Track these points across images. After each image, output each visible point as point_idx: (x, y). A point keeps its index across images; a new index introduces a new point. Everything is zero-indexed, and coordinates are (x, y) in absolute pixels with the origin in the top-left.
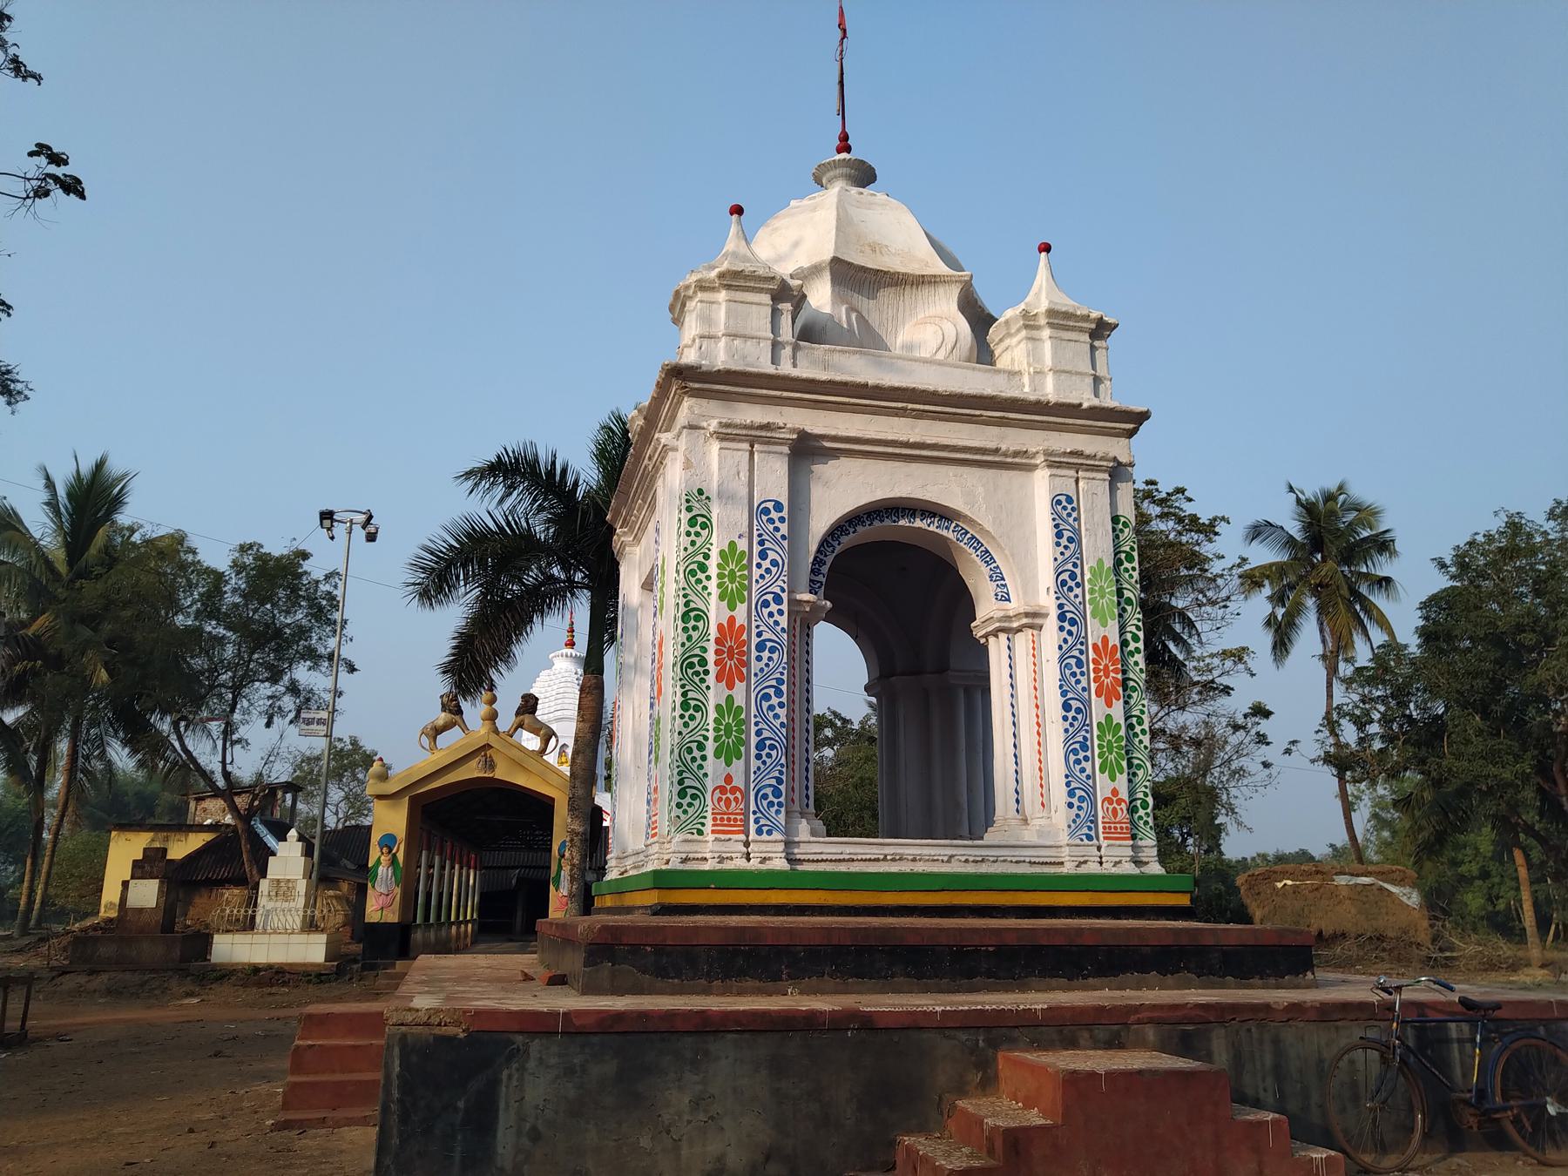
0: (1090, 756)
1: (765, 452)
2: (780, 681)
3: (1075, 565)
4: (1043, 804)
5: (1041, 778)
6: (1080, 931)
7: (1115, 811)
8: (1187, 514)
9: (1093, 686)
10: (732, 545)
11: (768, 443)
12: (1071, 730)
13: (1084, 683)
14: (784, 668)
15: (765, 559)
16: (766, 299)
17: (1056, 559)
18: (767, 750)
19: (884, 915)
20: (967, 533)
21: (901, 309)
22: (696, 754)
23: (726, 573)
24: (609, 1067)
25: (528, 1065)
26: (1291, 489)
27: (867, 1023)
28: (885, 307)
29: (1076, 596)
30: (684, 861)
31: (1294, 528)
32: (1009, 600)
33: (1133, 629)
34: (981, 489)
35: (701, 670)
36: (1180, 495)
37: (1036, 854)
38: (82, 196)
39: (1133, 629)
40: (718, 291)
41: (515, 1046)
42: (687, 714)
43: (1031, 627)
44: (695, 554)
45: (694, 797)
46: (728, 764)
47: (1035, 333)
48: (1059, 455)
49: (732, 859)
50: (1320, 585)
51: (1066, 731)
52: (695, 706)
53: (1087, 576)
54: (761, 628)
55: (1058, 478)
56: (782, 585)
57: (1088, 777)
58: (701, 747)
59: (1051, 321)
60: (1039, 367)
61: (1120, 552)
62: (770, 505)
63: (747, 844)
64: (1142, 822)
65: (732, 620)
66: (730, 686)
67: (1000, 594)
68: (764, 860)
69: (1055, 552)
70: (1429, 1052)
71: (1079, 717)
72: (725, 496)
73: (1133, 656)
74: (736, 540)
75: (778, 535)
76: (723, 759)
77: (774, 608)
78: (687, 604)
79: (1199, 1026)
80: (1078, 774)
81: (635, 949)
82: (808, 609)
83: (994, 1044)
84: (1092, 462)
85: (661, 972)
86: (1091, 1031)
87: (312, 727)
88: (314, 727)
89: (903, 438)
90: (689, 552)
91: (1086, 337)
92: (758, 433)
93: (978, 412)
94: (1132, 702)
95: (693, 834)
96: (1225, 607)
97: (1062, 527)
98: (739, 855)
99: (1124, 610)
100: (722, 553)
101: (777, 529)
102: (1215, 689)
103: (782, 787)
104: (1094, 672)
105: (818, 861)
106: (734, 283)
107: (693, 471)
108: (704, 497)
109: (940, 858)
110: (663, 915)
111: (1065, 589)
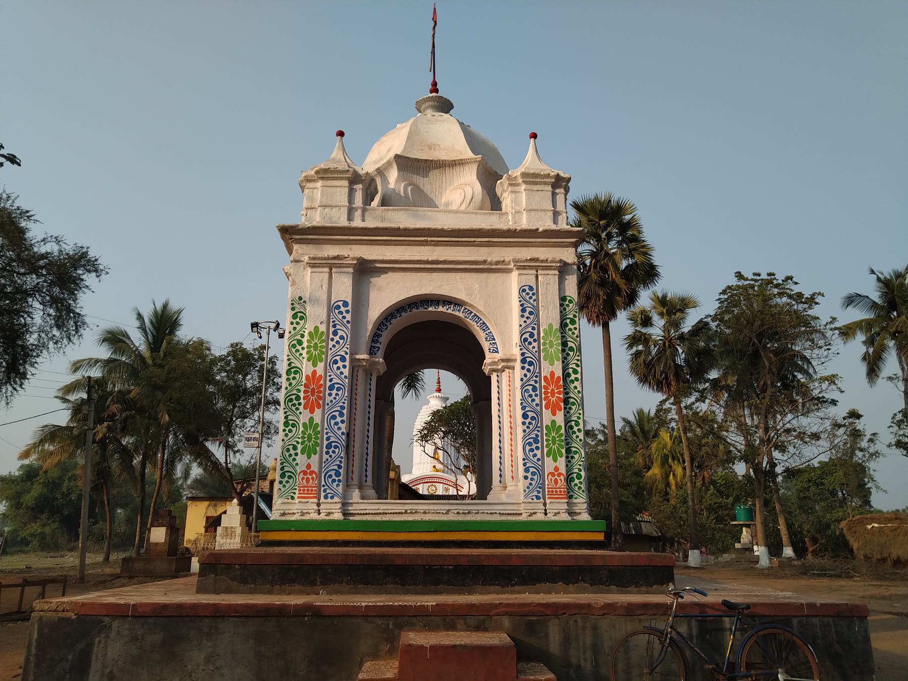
0: (540, 446)
1: (339, 272)
2: (342, 408)
3: (533, 328)
4: (512, 477)
5: (512, 461)
6: (510, 556)
8: (795, 292)
9: (544, 403)
10: (316, 328)
11: (340, 267)
12: (528, 430)
14: (345, 400)
15: (336, 335)
16: (345, 183)
17: (521, 326)
18: (333, 449)
19: (398, 546)
20: (471, 312)
21: (444, 181)
22: (292, 452)
23: (312, 345)
24: (158, 637)
25: (110, 635)
26: (873, 272)
27: (316, 612)
28: (434, 181)
29: (534, 347)
30: (284, 514)
31: (875, 294)
33: (574, 366)
34: (477, 286)
35: (297, 403)
36: (790, 281)
37: (503, 508)
38: (19, 165)
39: (574, 366)
40: (318, 182)
41: (104, 624)
42: (287, 429)
43: (508, 368)
44: (296, 335)
45: (290, 477)
46: (309, 457)
47: (516, 188)
48: (524, 262)
49: (309, 514)
50: (896, 332)
51: (524, 431)
52: (293, 424)
53: (542, 334)
54: (332, 377)
56: (346, 350)
57: (538, 460)
58: (295, 448)
59: (525, 180)
62: (340, 304)
63: (319, 505)
64: (577, 487)
65: (314, 373)
66: (312, 412)
67: (492, 349)
68: (329, 514)
69: (520, 321)
70: (708, 637)
71: (534, 422)
72: (315, 301)
73: (573, 383)
74: (319, 325)
75: (345, 321)
76: (306, 454)
77: (340, 364)
78: (289, 365)
80: (532, 458)
81: (229, 566)
82: (364, 364)
83: (400, 627)
84: (545, 264)
85: (244, 581)
86: (464, 619)
87: (250, 442)
88: (252, 442)
89: (425, 258)
90: (292, 334)
91: (549, 188)
92: (333, 262)
93: (472, 239)
95: (288, 499)
96: (829, 349)
97: (525, 306)
98: (313, 511)
99: (568, 354)
100: (310, 333)
101: (344, 317)
102: (825, 402)
103: (341, 471)
105: (364, 514)
108: (302, 301)
109: (441, 511)
111: (526, 343)
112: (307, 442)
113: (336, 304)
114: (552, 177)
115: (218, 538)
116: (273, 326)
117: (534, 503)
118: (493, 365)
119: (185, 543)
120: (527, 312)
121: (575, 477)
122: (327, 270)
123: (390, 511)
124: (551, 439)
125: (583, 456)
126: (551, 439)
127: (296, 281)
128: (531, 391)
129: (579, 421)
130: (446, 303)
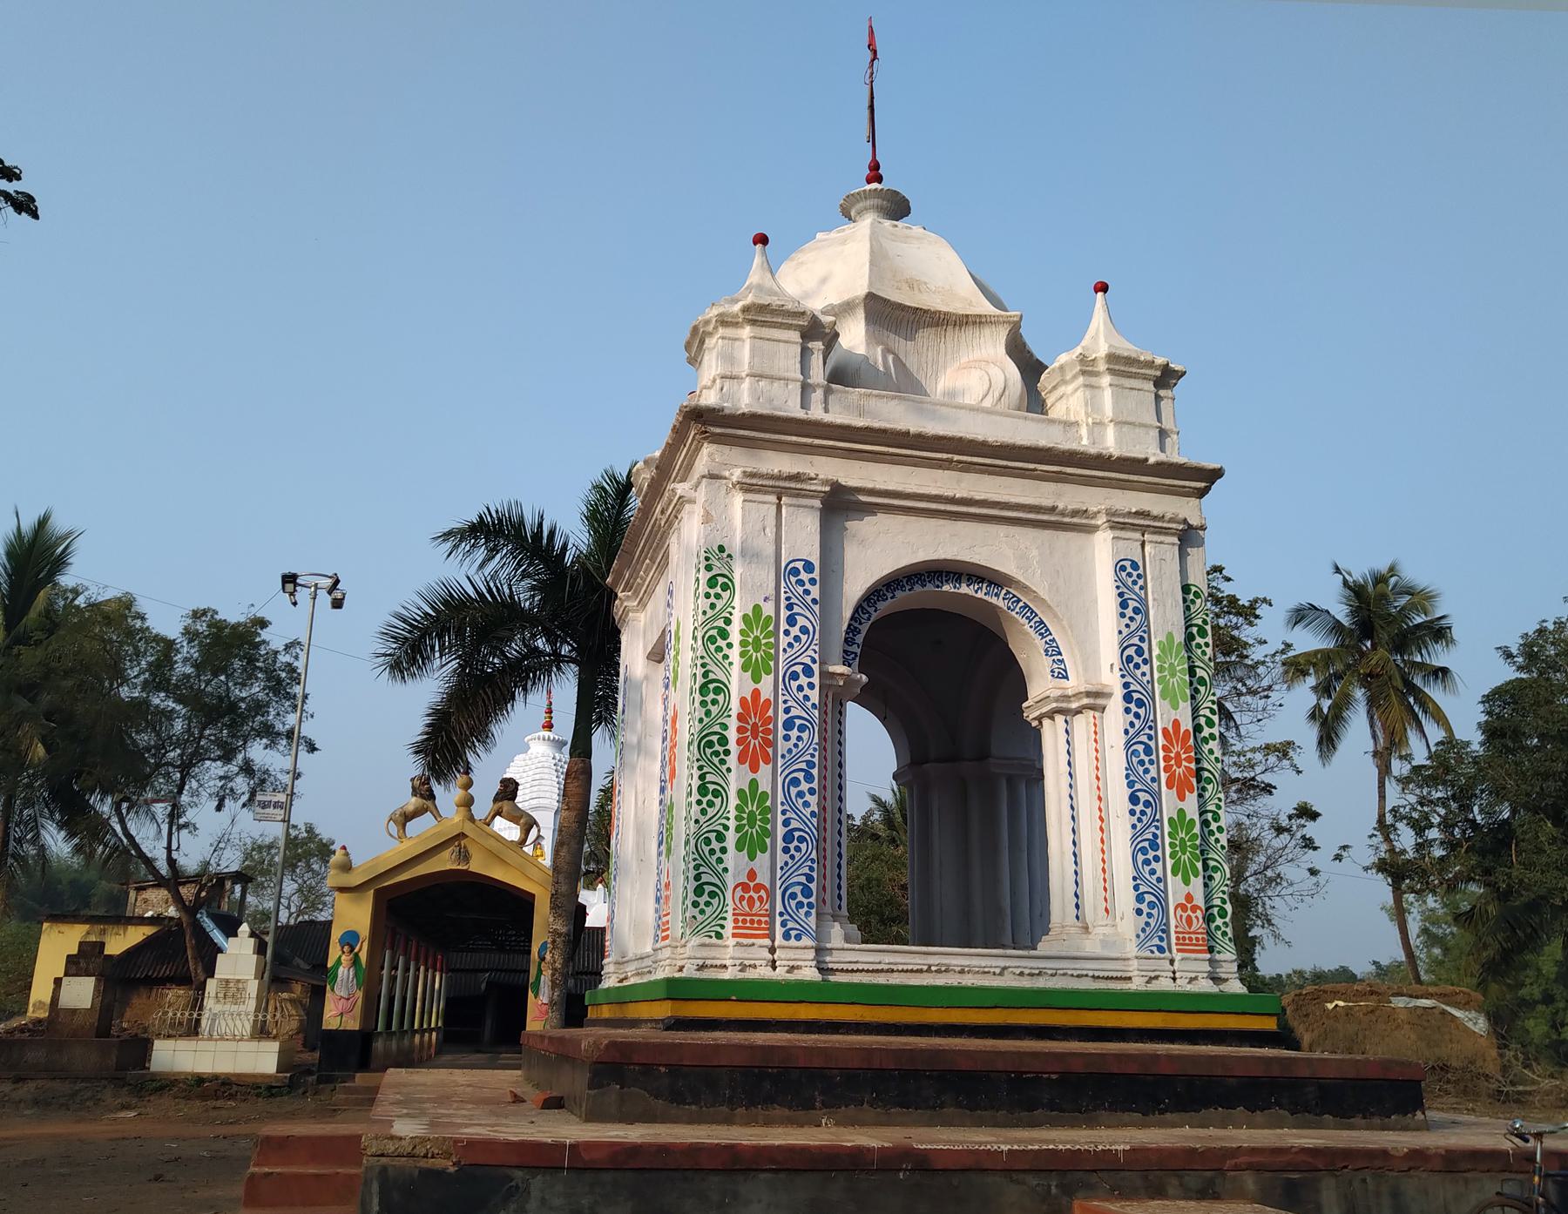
2: (810, 764)
3: (1142, 639)
5: (1105, 880)
6: (1155, 1057)
7: (1189, 919)
8: (1225, 595)
10: (757, 608)
11: (797, 496)
12: (1139, 826)
13: (1153, 773)
14: (815, 749)
15: (794, 625)
16: (795, 336)
17: (1120, 632)
20: (1019, 601)
23: (750, 640)
26: (1338, 570)
27: (922, 1163)
28: (925, 348)
29: (1144, 674)
30: (701, 968)
31: (1341, 613)
32: (1067, 678)
34: (1035, 552)
35: (721, 749)
36: (1218, 574)
38: (35, 215)
40: (742, 327)
41: (513, 1184)
42: (705, 800)
44: (715, 618)
45: (712, 895)
46: (752, 857)
47: (1093, 380)
49: (755, 967)
50: (1370, 675)
51: (1134, 826)
53: (1156, 652)
54: (789, 704)
55: (1121, 542)
56: (813, 655)
57: (1159, 880)
58: (721, 838)
59: (1112, 367)
60: (1098, 418)
61: (1191, 625)
62: (800, 565)
63: (772, 950)
64: (1219, 933)
65: (756, 693)
66: (754, 768)
67: (1057, 670)
68: (792, 969)
69: (1119, 624)
71: (1148, 811)
72: (749, 554)
73: (1207, 744)
74: (761, 603)
75: (809, 599)
78: (705, 675)
79: (1306, 1174)
80: (1147, 876)
81: (648, 1069)
82: (841, 683)
83: (1069, 1191)
84: (1159, 524)
85: (677, 1097)
87: (267, 811)
88: (270, 810)
89: (950, 493)
91: (1150, 386)
92: (787, 484)
93: (1032, 466)
94: (1207, 795)
95: (711, 937)
96: (1267, 697)
97: (1126, 596)
98: (764, 963)
99: (1197, 691)
100: (745, 618)
101: (807, 592)
102: (1255, 787)
103: (813, 886)
104: (1165, 761)
105: (852, 971)
106: (760, 319)
107: (713, 525)
108: (725, 555)
109: (992, 970)
110: (677, 1030)
111: (1131, 665)
112: (747, 828)
113: (791, 565)
114: (1156, 368)
115: (209, 1003)
116: (328, 582)
117: (1155, 959)
118: (1063, 701)
119: (31, 1009)
120: (1130, 608)
121: (1216, 913)
122: (773, 498)
123: (900, 968)
124: (1177, 843)
125: (1228, 876)
126: (1177, 843)
127: (713, 513)
128: (1142, 754)
129: (1219, 812)
130: (974, 579)
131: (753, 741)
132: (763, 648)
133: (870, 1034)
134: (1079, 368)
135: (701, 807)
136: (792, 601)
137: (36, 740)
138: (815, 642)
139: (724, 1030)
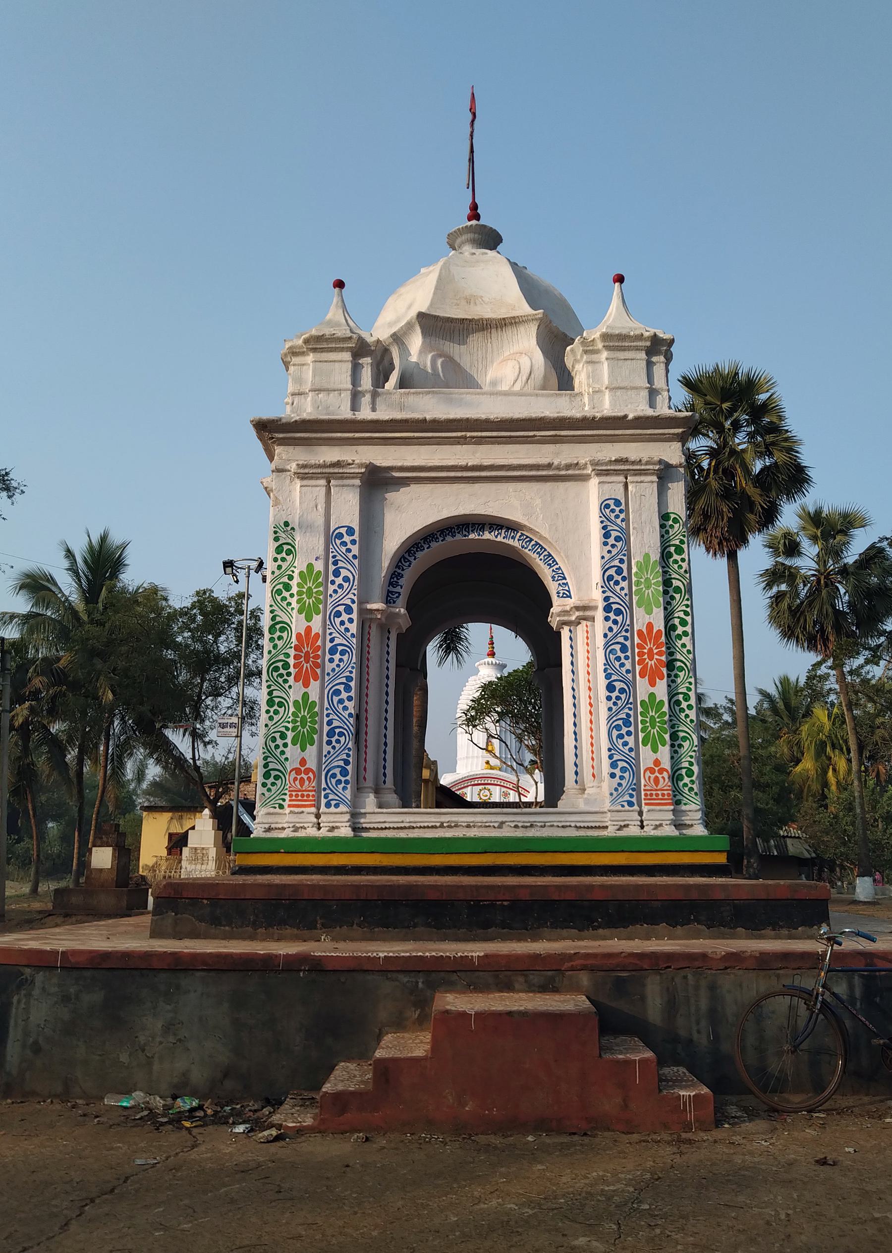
0: (633, 731)
1: (339, 486)
2: (349, 679)
3: (621, 561)
4: (594, 775)
6: (590, 887)
7: (656, 780)
9: (638, 668)
10: (310, 566)
11: (342, 478)
12: (614, 708)
13: (628, 666)
14: (353, 668)
16: (347, 356)
17: (603, 557)
18: (336, 737)
19: (431, 874)
20: (531, 540)
21: (490, 350)
22: (279, 742)
23: (304, 590)
24: (96, 997)
27: (316, 966)
28: (475, 350)
29: (622, 589)
30: (269, 830)
32: (570, 597)
33: (682, 615)
34: (538, 501)
35: (284, 672)
37: (580, 819)
39: (682, 615)
40: (308, 355)
42: (272, 710)
43: (585, 619)
44: (281, 576)
45: (277, 777)
46: (303, 749)
47: (594, 357)
48: (606, 464)
49: (305, 828)
51: (610, 709)
52: (280, 702)
53: (634, 570)
54: (334, 635)
55: (606, 485)
56: (353, 597)
57: (631, 750)
58: (283, 736)
60: (597, 386)
61: (670, 546)
62: (343, 531)
63: (318, 816)
64: (686, 789)
65: (308, 629)
66: (306, 685)
67: (562, 592)
68: (332, 829)
69: (602, 550)
70: (878, 1000)
71: (623, 696)
72: (306, 527)
74: (314, 562)
75: (350, 555)
76: (298, 745)
77: (345, 617)
78: (273, 619)
79: (634, 973)
80: (621, 747)
82: (379, 616)
84: (638, 467)
85: (215, 921)
86: (526, 976)
87: (225, 730)
88: (228, 729)
89: (463, 463)
90: (275, 575)
91: (643, 355)
92: (331, 470)
93: (531, 434)
95: (275, 808)
97: (609, 528)
98: (310, 825)
99: (672, 598)
101: (349, 550)
103: (349, 768)
104: (638, 656)
105: (382, 829)
106: (318, 346)
107: (280, 507)
108: (289, 528)
109: (492, 824)
110: (241, 874)
111: (612, 583)
112: (300, 728)
113: (337, 531)
114: (646, 340)
116: (254, 565)
117: (625, 811)
118: (564, 616)
119: (141, 870)
120: (612, 538)
121: (684, 774)
122: (323, 482)
123: (418, 825)
124: (648, 720)
125: (696, 743)
126: (648, 720)
127: (280, 498)
128: (619, 652)
129: (689, 693)
130: (495, 527)
131: (305, 665)
132: (314, 595)
133: (385, 874)
134: (581, 349)
135: (269, 715)
136: (337, 558)
137: (107, 689)
138: (354, 587)
139: (274, 874)
